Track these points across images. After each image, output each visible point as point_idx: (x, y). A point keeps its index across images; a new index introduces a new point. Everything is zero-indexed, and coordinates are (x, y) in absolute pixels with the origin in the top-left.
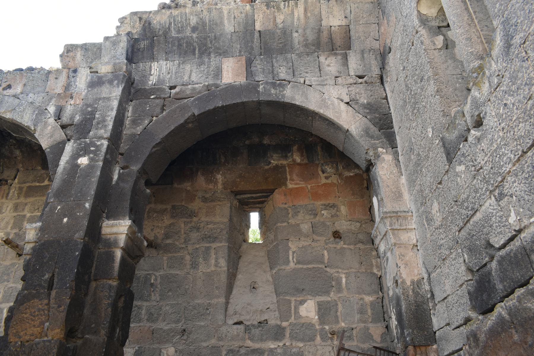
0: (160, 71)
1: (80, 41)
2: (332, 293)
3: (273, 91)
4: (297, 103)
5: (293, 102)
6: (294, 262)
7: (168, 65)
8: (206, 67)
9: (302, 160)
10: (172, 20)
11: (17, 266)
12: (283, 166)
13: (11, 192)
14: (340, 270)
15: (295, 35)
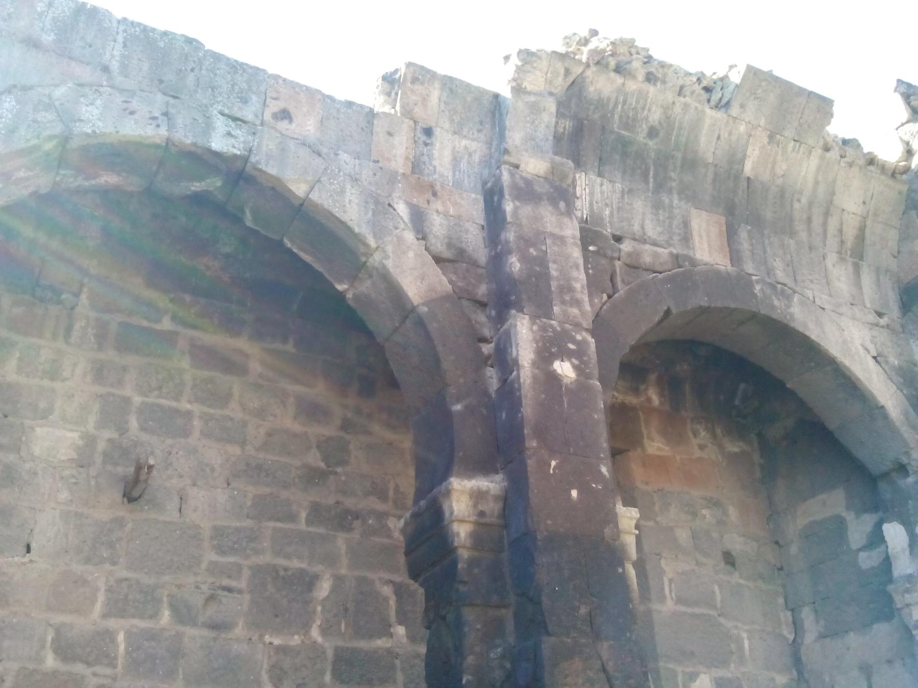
0: (592, 194)
1: (442, 69)
2: (733, 665)
3: (776, 303)
4: (813, 337)
5: (807, 333)
6: (672, 598)
7: (604, 187)
8: (667, 215)
9: (661, 403)
10: (621, 99)
11: (130, 526)
12: (633, 409)
13: (77, 326)
14: (739, 625)
15: (797, 205)
